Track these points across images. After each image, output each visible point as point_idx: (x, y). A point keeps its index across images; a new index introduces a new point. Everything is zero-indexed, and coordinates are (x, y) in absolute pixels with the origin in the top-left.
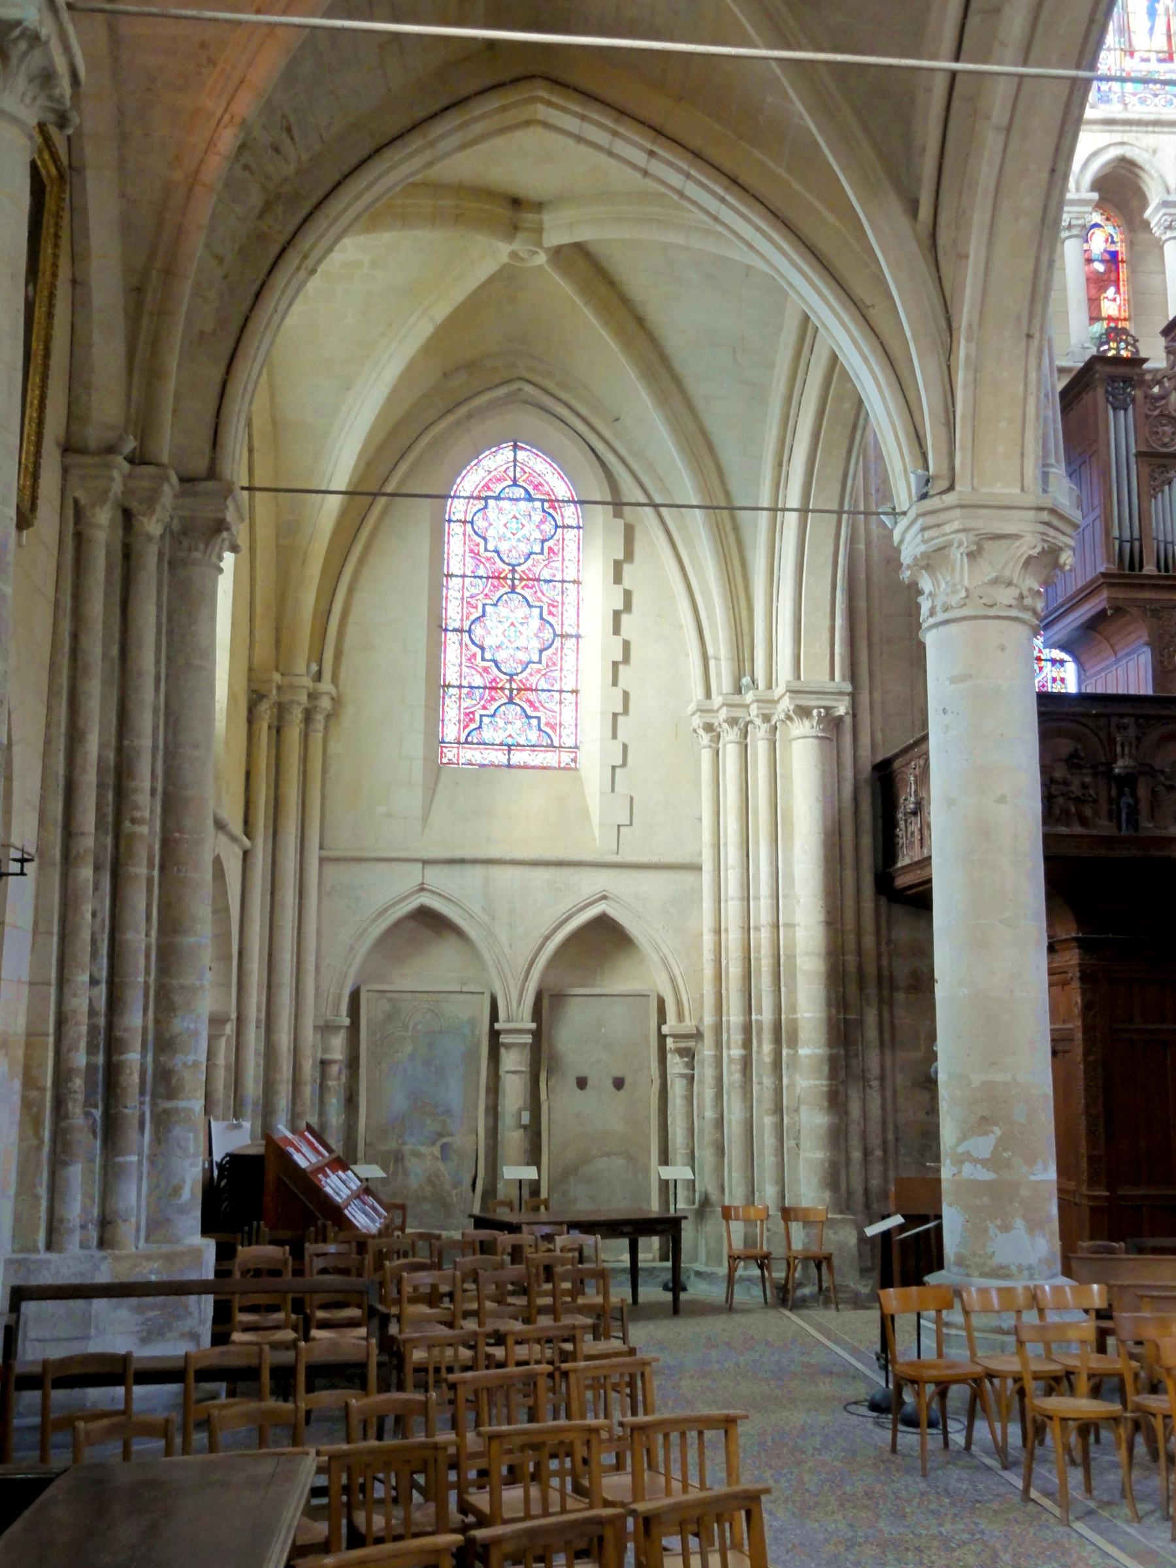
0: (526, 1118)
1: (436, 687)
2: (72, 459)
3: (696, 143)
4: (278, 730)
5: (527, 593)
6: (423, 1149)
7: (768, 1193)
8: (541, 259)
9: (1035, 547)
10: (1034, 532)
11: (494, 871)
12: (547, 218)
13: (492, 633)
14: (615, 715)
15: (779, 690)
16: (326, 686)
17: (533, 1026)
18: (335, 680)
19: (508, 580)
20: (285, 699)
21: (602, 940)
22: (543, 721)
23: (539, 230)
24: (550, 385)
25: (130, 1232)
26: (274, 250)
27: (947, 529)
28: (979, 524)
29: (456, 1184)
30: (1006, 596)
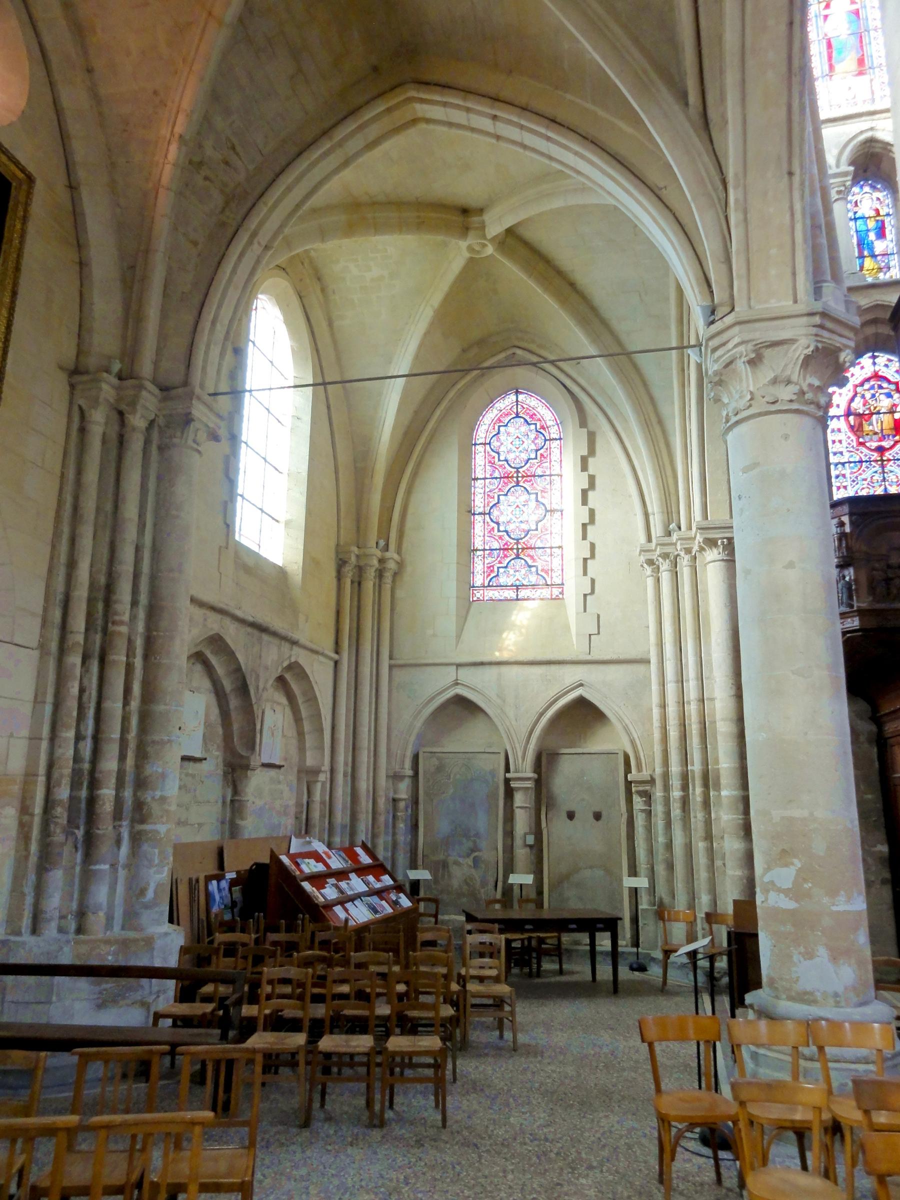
0: (531, 840)
1: (467, 551)
2: (77, 378)
3: (523, 100)
4: (358, 584)
5: (527, 485)
6: (461, 860)
7: (704, 901)
8: (490, 250)
9: (808, 347)
10: (806, 335)
11: (504, 669)
12: (487, 217)
13: (504, 513)
14: (585, 560)
16: (392, 554)
17: (536, 776)
18: (399, 551)
20: (362, 563)
21: (582, 714)
22: (540, 568)
23: (482, 227)
24: (533, 347)
26: (230, 231)
27: (730, 345)
28: (757, 335)
29: (484, 884)
30: (786, 393)
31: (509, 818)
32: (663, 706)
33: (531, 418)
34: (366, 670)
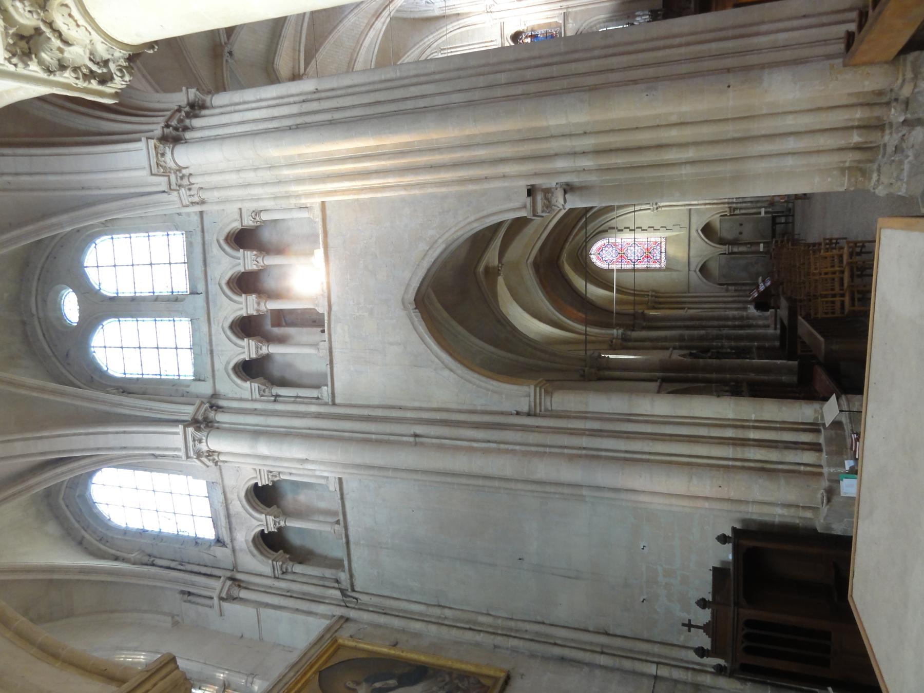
1: (647, 270)
4: (660, 303)
11: (691, 254)
16: (650, 294)
19: (622, 256)
21: (708, 230)
25: (766, 322)
32: (705, 204)
33: (600, 249)
34: (691, 299)
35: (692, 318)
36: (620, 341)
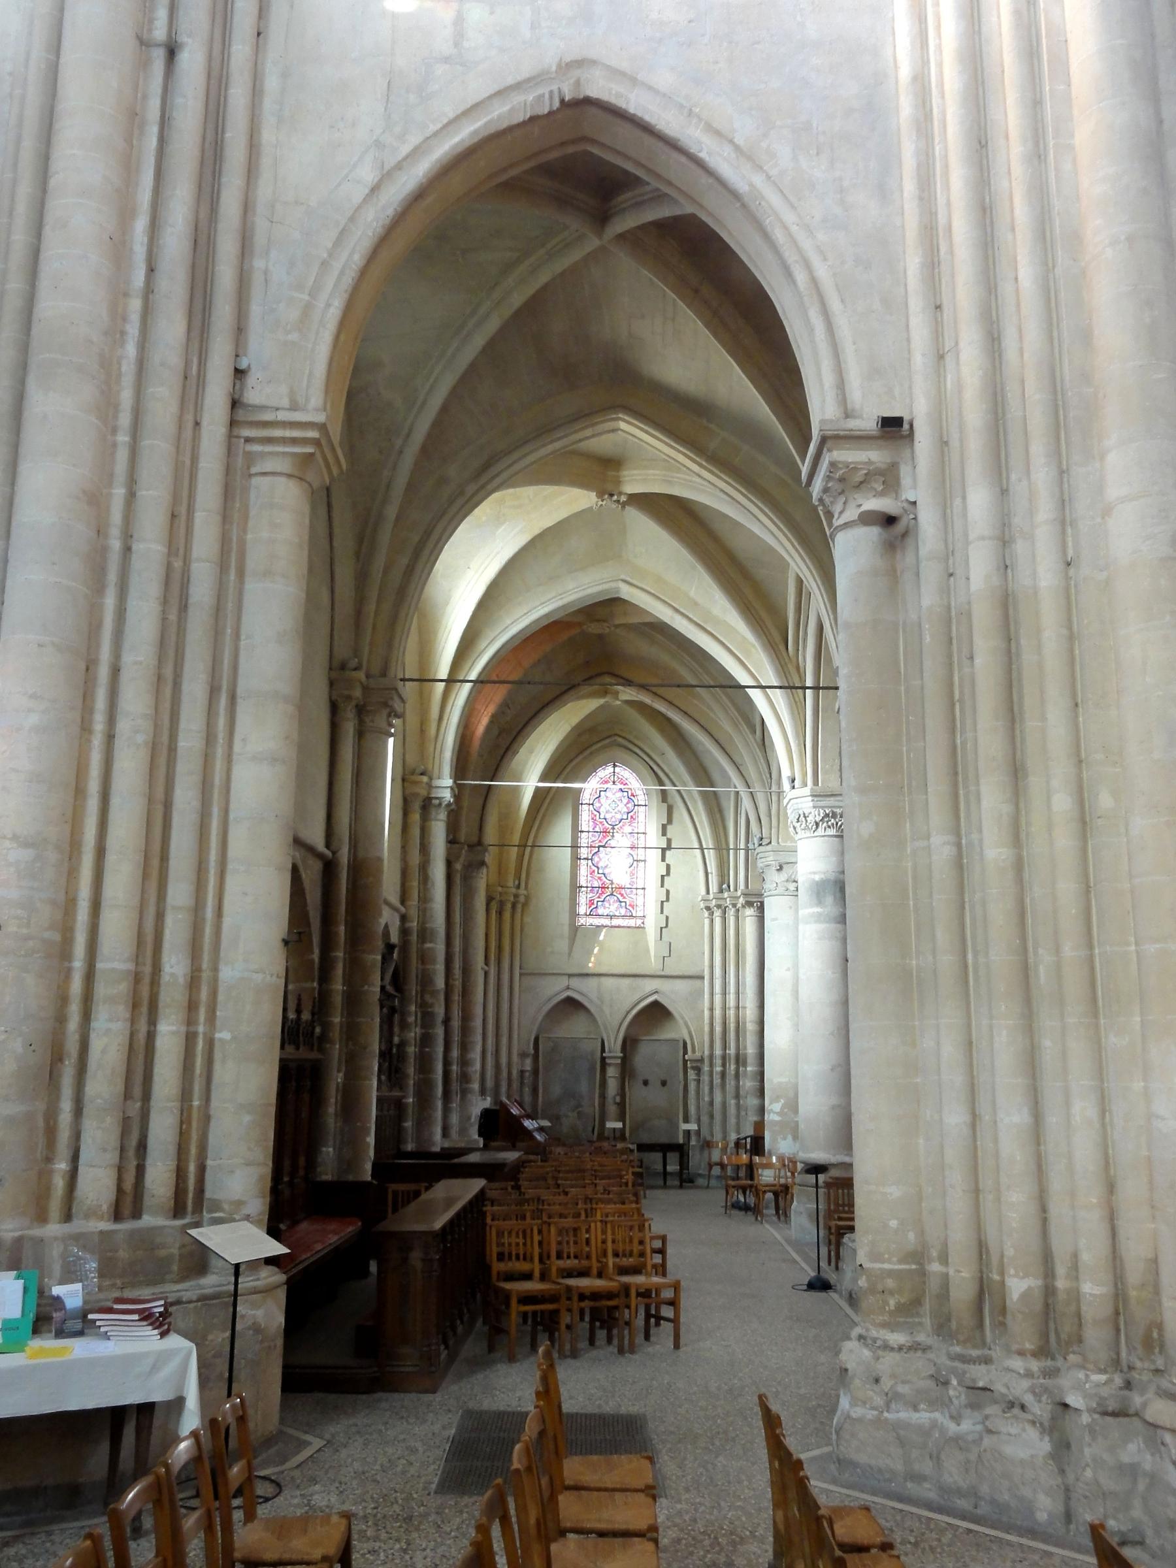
0: (618, 1099)
1: (575, 887)
4: (500, 913)
11: (603, 979)
15: (739, 893)
16: (522, 891)
21: (656, 1013)
24: (631, 738)
31: (603, 1083)
32: (712, 1009)
35: (466, 971)
36: (424, 793)
